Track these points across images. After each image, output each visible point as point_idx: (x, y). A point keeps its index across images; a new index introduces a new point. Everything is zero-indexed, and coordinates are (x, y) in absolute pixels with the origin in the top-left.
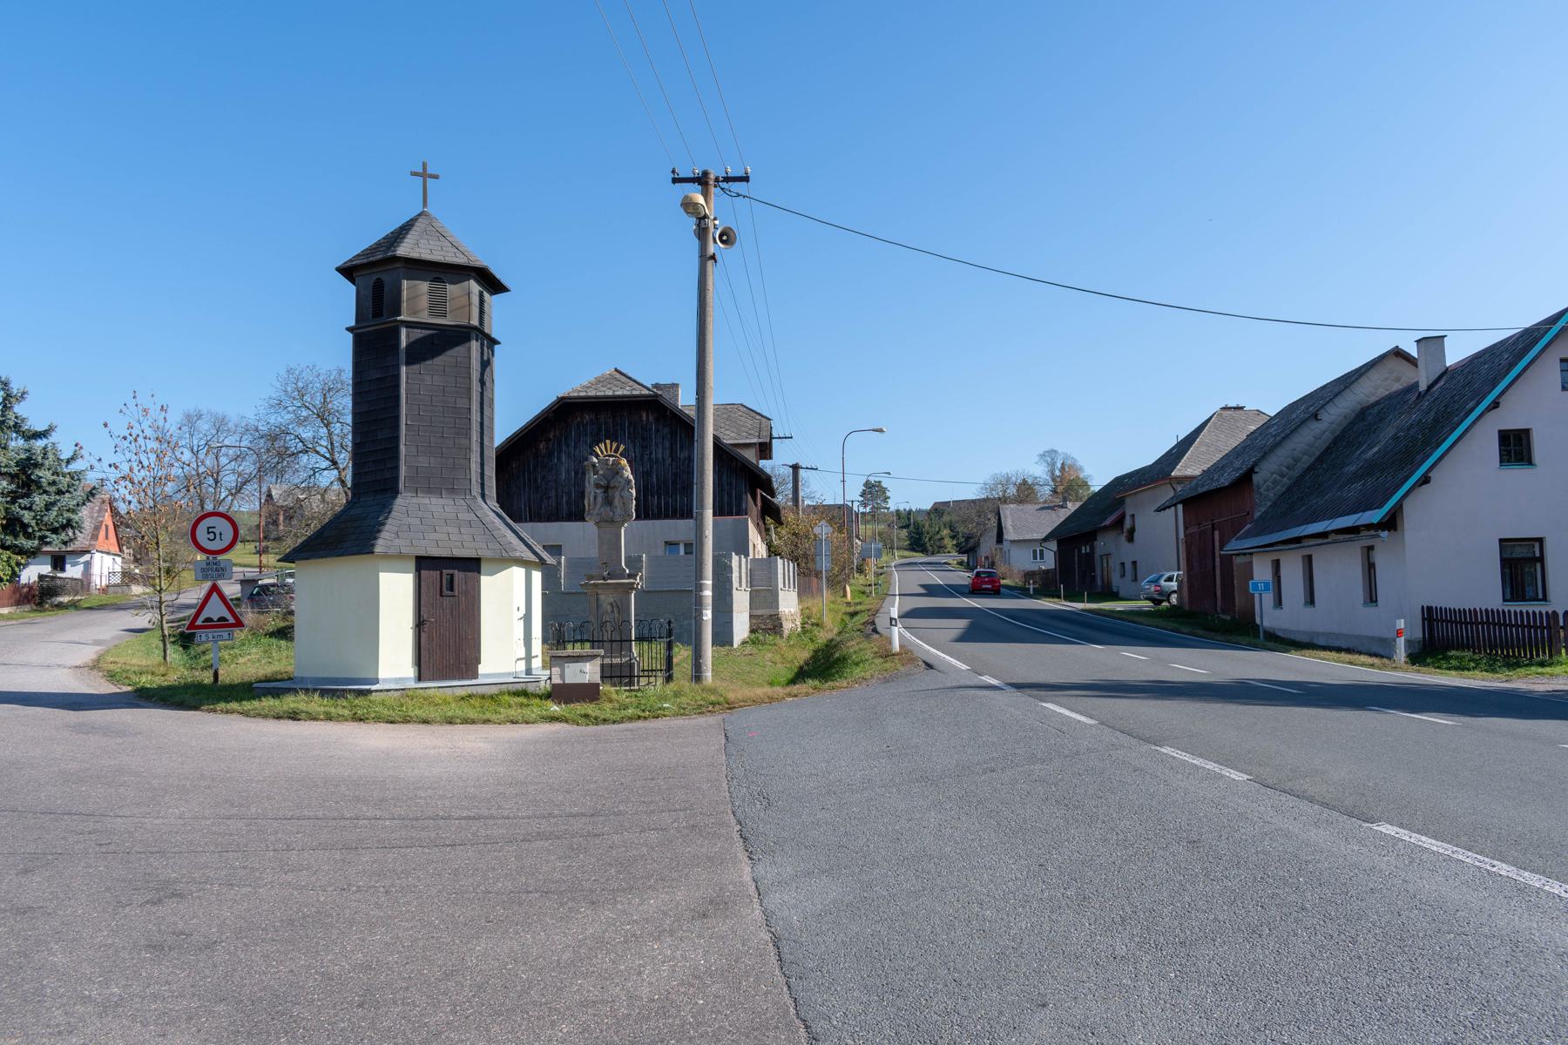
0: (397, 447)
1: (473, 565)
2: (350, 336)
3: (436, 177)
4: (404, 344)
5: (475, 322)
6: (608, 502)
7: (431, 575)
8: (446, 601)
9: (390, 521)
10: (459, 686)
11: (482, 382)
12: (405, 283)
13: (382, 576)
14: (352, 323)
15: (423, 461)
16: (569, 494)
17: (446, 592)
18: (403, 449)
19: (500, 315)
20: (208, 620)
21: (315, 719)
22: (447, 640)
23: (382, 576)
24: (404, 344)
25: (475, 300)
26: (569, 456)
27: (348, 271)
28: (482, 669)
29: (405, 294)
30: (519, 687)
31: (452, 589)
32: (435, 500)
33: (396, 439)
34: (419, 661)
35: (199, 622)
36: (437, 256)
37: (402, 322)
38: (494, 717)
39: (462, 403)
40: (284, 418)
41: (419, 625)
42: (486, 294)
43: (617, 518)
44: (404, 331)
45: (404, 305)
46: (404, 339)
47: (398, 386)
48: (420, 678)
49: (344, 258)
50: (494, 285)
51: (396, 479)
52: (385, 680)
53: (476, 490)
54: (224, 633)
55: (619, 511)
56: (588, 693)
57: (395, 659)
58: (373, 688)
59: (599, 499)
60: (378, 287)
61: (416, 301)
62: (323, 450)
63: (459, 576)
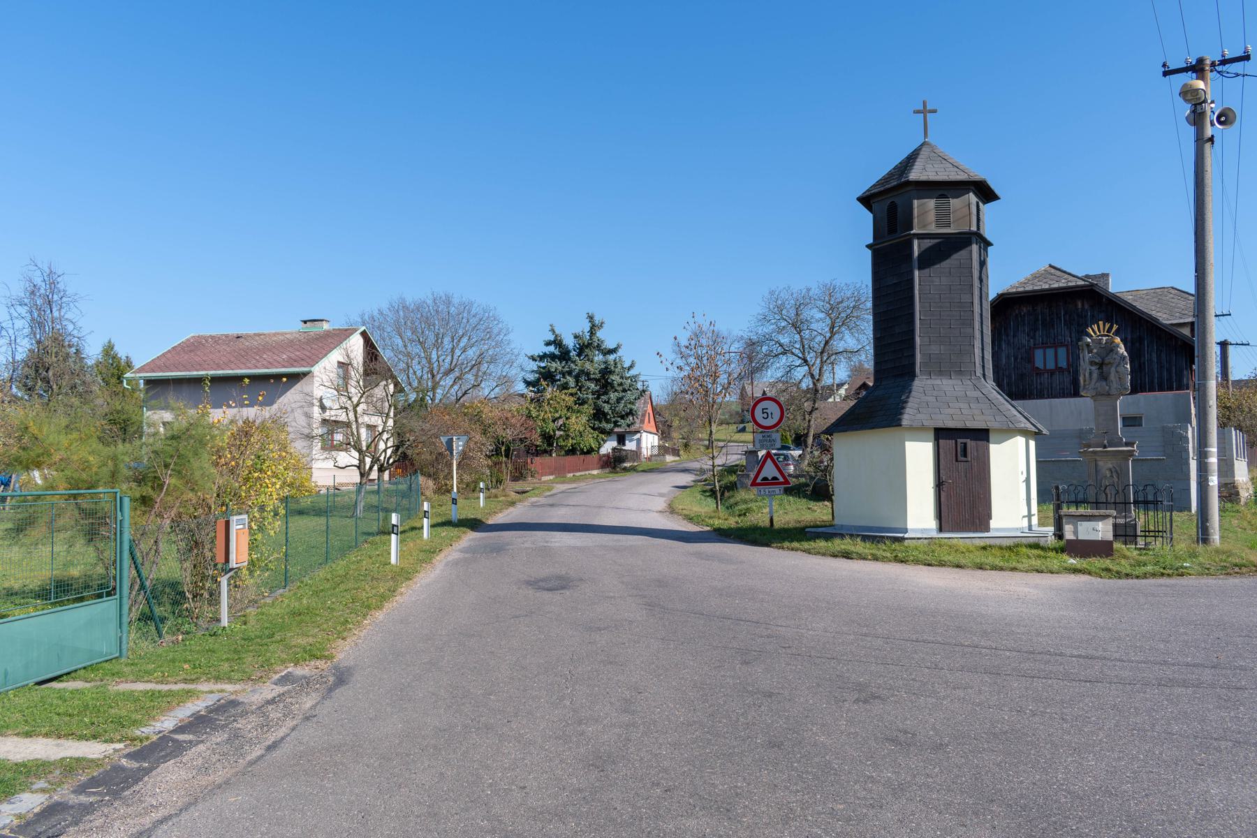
0: (913, 339)
1: (983, 435)
3: (934, 111)
4: (916, 254)
5: (974, 228)
6: (1104, 377)
7: (947, 444)
9: (911, 399)
11: (981, 280)
13: (908, 444)
15: (935, 349)
16: (1009, 377)
17: (960, 458)
18: (918, 340)
19: (992, 220)
20: (765, 479)
22: (964, 499)
24: (916, 254)
26: (1008, 344)
27: (866, 200)
28: (993, 524)
30: (1031, 540)
31: (965, 455)
32: (945, 381)
33: (912, 332)
34: (939, 515)
35: (759, 481)
36: (942, 177)
38: (1019, 566)
40: (769, 328)
41: (939, 485)
43: (1113, 392)
44: (916, 242)
45: (915, 221)
48: (941, 530)
51: (914, 364)
53: (979, 372)
55: (1115, 385)
57: (920, 514)
59: (1095, 376)
60: (893, 208)
61: (926, 216)
62: (797, 352)
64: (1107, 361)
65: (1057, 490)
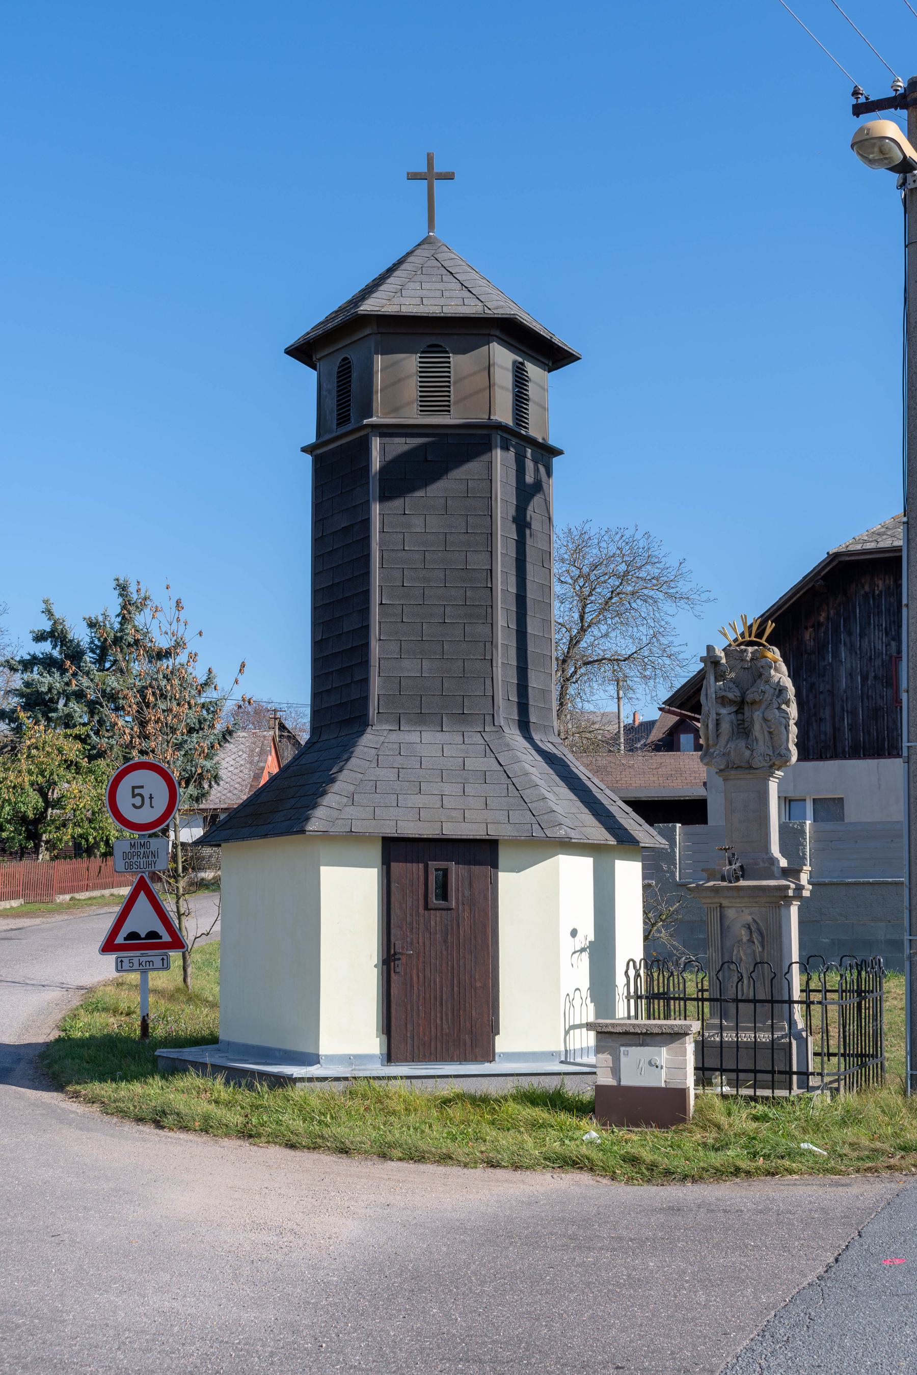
0: (365, 647)
1: (483, 853)
2: (308, 459)
3: (449, 176)
4: (376, 464)
5: (504, 414)
6: (743, 730)
7: (408, 871)
8: (435, 918)
9: (343, 776)
10: (453, 1075)
11: (521, 523)
12: (379, 361)
13: (325, 871)
14: (312, 439)
15: (410, 668)
16: (853, 713)
17: (434, 901)
18: (375, 648)
19: (559, 405)
20: (133, 935)
21: (185, 1128)
22: (440, 986)
23: (325, 871)
24: (376, 464)
25: (504, 379)
26: (851, 649)
27: (304, 351)
28: (502, 1044)
29: (378, 379)
30: (551, 1084)
32: (429, 736)
33: (365, 630)
34: (387, 1027)
35: (120, 940)
36: (431, 308)
37: (374, 426)
38: (458, 1150)
39: (478, 561)
41: (389, 960)
42: (532, 370)
43: (758, 762)
44: (376, 443)
45: (378, 398)
46: (378, 454)
47: (367, 539)
48: (390, 1057)
49: (294, 336)
50: (554, 356)
51: (365, 699)
52: (332, 1059)
53: (506, 712)
54: (154, 956)
55: (762, 747)
56: (660, 1108)
57: (347, 1021)
58: (296, 1071)
59: (725, 727)
60: (345, 371)
61: (397, 384)
63: (456, 871)
64: (749, 697)
65: (709, 959)
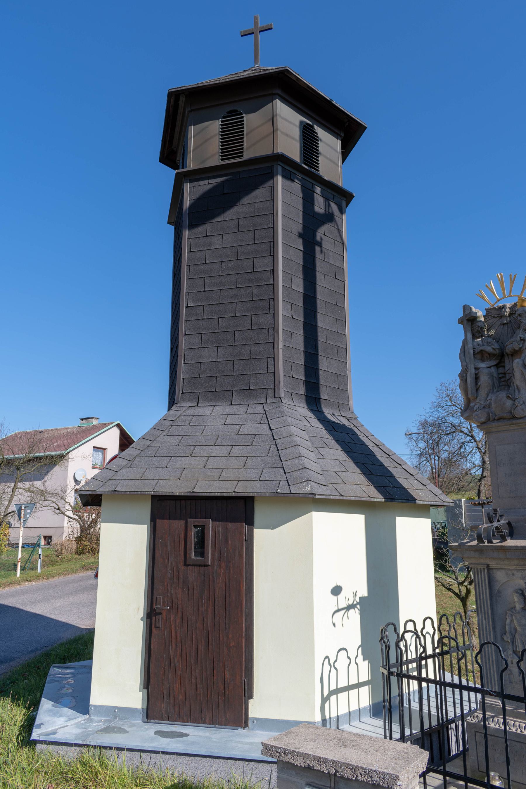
1: (239, 511)
15: (208, 355)
28: (256, 709)
31: (202, 554)
32: (221, 409)
34: (149, 681)
39: (262, 264)
40: (442, 413)
41: (152, 615)
48: (151, 713)
62: (466, 430)
64: (508, 349)
